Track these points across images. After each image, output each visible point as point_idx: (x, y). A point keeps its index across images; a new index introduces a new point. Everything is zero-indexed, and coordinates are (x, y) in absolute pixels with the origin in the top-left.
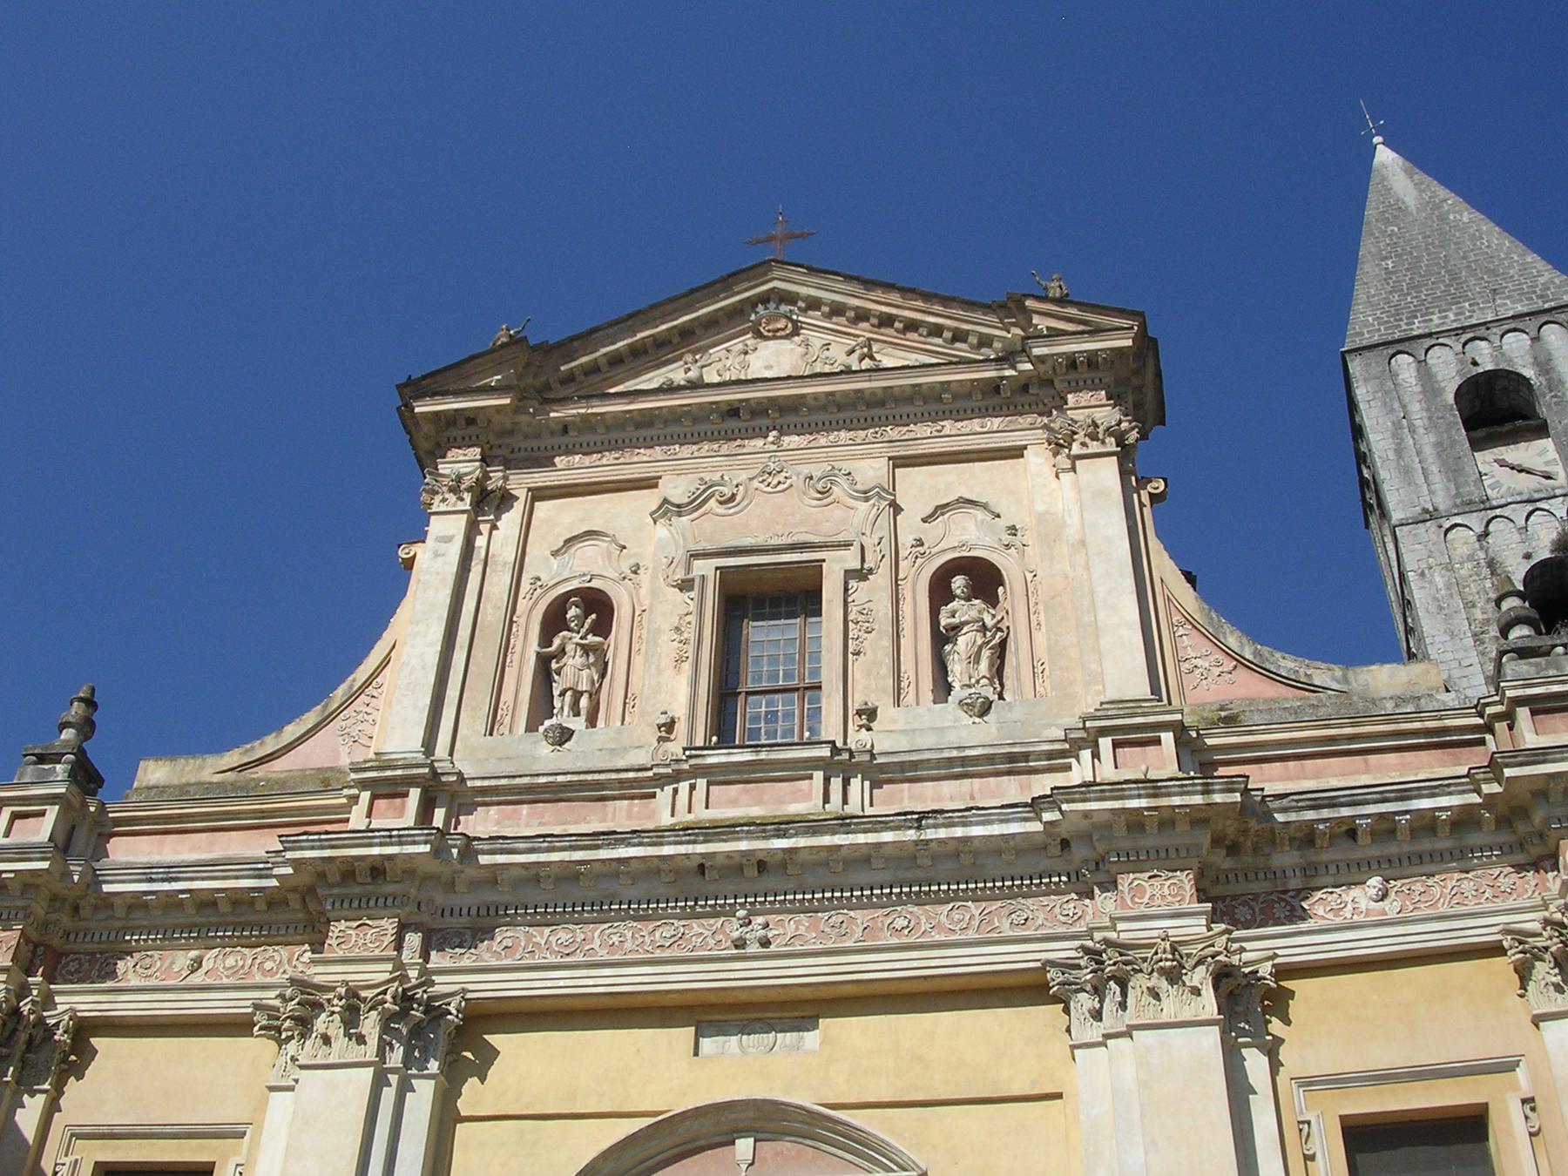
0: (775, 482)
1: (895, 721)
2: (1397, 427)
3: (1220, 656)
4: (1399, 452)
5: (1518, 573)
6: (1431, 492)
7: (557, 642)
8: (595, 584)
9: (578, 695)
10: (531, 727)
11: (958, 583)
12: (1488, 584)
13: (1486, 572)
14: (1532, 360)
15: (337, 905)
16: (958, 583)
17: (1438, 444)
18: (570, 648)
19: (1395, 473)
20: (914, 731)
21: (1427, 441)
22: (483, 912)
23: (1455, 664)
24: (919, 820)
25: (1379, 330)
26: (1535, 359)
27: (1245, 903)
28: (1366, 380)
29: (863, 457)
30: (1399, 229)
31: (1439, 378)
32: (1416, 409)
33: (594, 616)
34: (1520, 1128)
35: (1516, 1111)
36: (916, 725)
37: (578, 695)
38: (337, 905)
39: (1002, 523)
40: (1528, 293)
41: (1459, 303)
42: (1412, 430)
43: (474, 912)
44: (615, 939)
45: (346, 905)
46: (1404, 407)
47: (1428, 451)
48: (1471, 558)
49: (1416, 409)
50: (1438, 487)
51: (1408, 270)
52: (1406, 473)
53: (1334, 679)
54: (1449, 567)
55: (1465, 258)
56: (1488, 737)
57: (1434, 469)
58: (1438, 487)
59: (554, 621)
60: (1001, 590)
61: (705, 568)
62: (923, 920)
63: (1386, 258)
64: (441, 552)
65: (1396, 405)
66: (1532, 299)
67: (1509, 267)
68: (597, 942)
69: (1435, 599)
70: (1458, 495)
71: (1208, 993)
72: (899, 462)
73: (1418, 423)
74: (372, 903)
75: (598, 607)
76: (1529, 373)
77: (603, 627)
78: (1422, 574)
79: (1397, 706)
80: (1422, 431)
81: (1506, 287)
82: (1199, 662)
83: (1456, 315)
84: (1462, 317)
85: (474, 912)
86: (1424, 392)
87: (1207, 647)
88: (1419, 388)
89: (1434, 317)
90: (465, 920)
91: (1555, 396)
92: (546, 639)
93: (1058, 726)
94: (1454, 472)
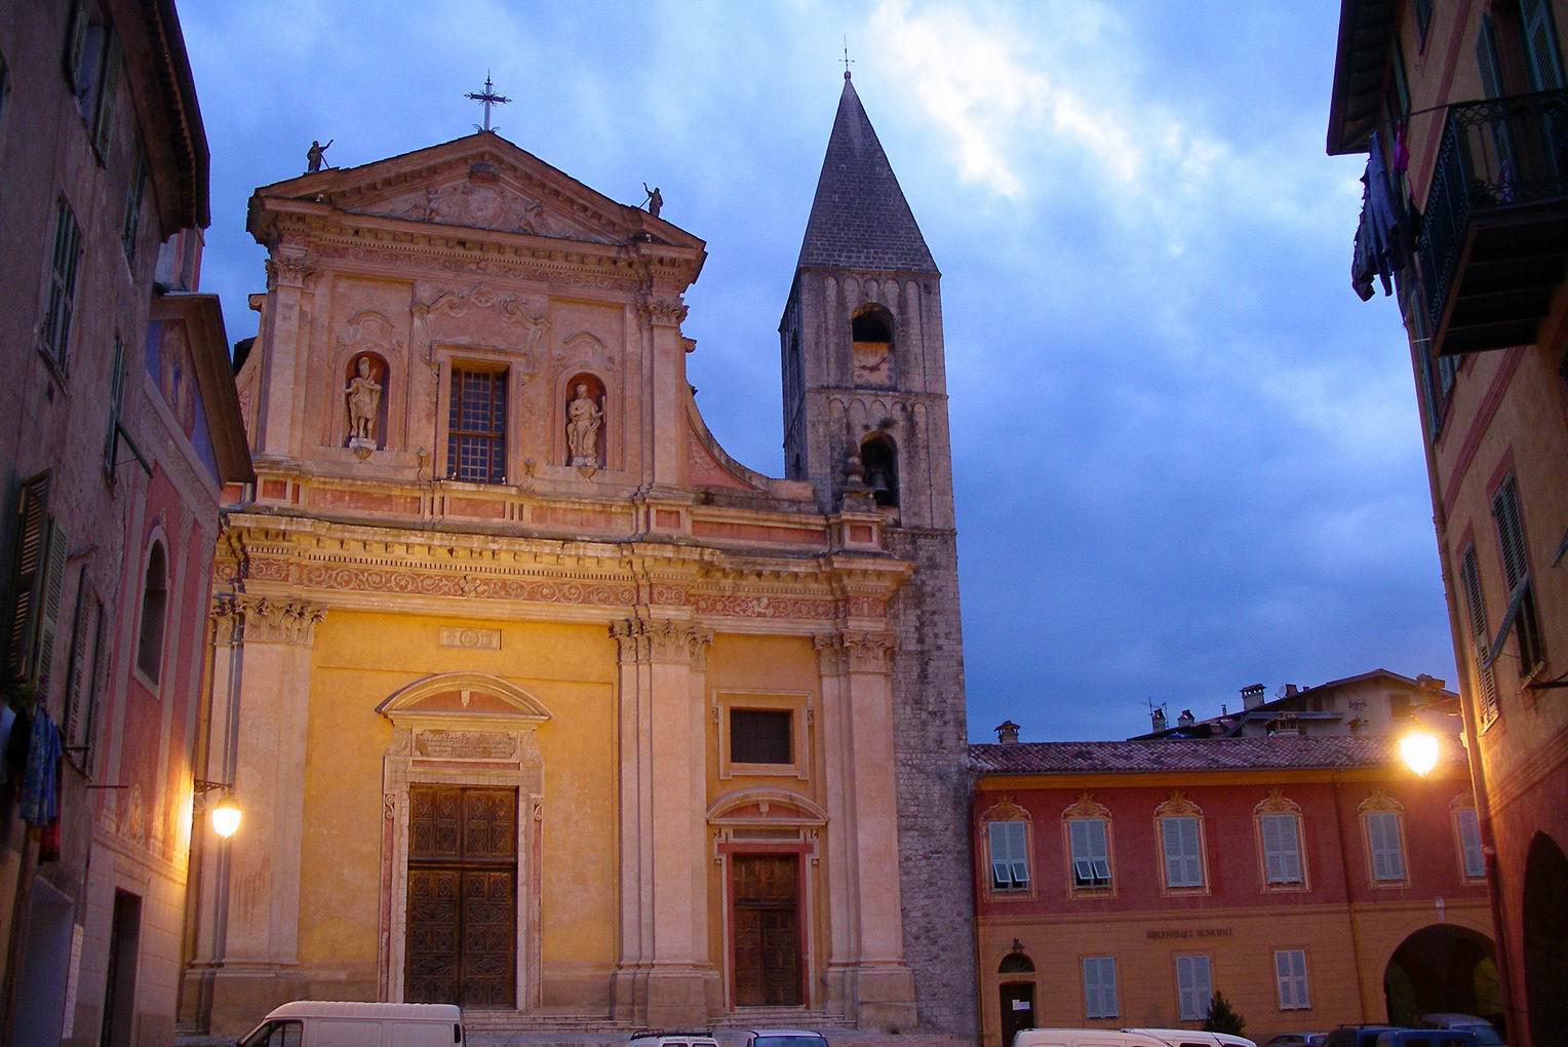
0: (483, 300)
1: (545, 474)
2: (819, 326)
3: (708, 459)
4: (817, 344)
5: (860, 437)
6: (829, 374)
7: (354, 386)
8: (376, 350)
9: (367, 420)
10: (346, 445)
11: (582, 389)
12: (844, 439)
13: (844, 431)
14: (896, 303)
15: (255, 550)
16: (582, 389)
17: (838, 344)
18: (361, 389)
19: (812, 357)
20: (556, 481)
21: (833, 340)
22: (332, 559)
23: (818, 482)
24: (563, 545)
25: (822, 255)
26: (899, 301)
27: (703, 600)
28: (809, 291)
29: (535, 292)
30: (847, 168)
31: (848, 299)
32: (831, 316)
33: (375, 370)
34: (805, 723)
35: (805, 714)
36: (555, 477)
37: (367, 420)
38: (255, 550)
39: (607, 353)
40: (906, 254)
41: (868, 248)
42: (827, 329)
43: (327, 558)
44: (403, 583)
45: (260, 550)
46: (825, 314)
47: (832, 346)
48: (839, 420)
49: (831, 316)
50: (832, 372)
51: (846, 208)
52: (818, 358)
53: (762, 483)
54: (827, 424)
55: (878, 210)
56: (828, 531)
57: (832, 360)
58: (832, 372)
59: (354, 372)
60: (604, 398)
61: (443, 356)
62: (557, 591)
63: (836, 193)
64: (287, 316)
65: (822, 312)
66: (906, 259)
67: (901, 228)
68: (393, 583)
69: (817, 442)
70: (841, 380)
71: (687, 649)
72: (555, 299)
73: (830, 326)
74: (275, 551)
75: (381, 366)
76: (894, 311)
77: (383, 377)
78: (814, 425)
79: (790, 506)
80: (831, 333)
81: (895, 244)
82: (698, 460)
83: (866, 258)
84: (868, 261)
85: (327, 558)
86: (837, 307)
87: (703, 454)
88: (835, 304)
89: (854, 255)
90: (321, 562)
91: (903, 331)
92: (348, 387)
93: (628, 491)
94: (843, 362)
